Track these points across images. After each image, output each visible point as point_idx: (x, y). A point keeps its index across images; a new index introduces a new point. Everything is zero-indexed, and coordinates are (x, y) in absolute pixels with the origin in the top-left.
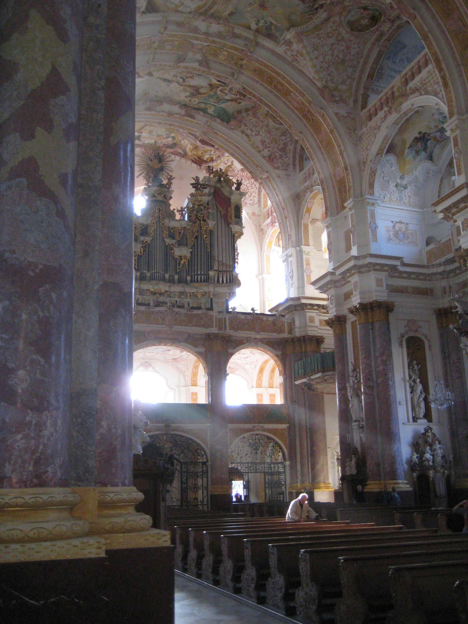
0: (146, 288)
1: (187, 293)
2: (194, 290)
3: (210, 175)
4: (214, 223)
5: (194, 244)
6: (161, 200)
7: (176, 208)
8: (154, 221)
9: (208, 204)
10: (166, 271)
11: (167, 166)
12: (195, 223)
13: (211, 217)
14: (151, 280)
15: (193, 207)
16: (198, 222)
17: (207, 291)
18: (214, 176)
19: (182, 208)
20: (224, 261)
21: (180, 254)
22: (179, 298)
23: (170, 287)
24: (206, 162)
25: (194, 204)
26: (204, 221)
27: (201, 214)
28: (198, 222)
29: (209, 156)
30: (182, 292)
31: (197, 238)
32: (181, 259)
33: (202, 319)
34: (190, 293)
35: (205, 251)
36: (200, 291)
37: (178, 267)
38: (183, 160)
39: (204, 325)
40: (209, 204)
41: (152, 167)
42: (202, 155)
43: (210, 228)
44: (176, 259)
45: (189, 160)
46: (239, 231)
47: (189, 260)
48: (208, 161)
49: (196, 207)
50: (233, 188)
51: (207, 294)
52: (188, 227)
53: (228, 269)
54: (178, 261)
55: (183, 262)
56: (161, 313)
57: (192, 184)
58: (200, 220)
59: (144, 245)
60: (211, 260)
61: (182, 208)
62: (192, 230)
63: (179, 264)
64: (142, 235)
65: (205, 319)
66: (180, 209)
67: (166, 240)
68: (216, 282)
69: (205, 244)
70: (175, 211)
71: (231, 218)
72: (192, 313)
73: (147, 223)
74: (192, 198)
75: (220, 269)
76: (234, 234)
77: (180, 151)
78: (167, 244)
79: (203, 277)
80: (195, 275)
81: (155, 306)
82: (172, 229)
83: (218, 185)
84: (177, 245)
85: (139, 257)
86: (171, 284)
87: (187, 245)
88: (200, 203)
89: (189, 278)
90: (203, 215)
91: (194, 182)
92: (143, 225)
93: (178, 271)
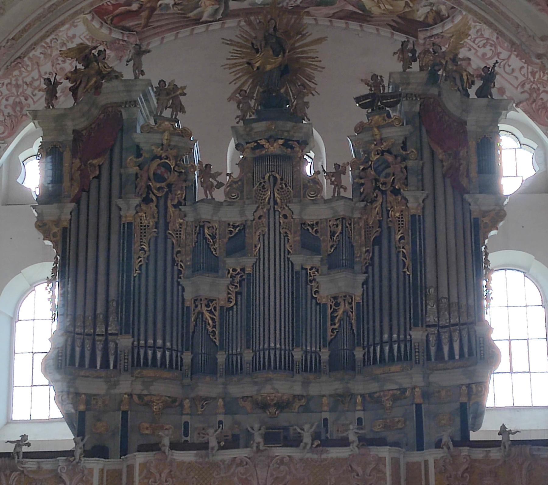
0: (241, 395)
1: (352, 396)
2: (373, 387)
3: (407, 64)
4: (421, 195)
5: (372, 259)
6: (278, 152)
7: (321, 170)
8: (260, 212)
9: (404, 148)
10: (296, 343)
11: (307, 58)
12: (372, 202)
13: (412, 180)
14: (254, 369)
15: (368, 159)
17: (405, 386)
18: (421, 69)
19: (337, 166)
20: (454, 299)
21: (334, 291)
22: (330, 411)
23: (306, 383)
24: (425, 25)
25: (367, 152)
26: (396, 192)
27: (387, 176)
28: (380, 199)
29: (427, 9)
30: (339, 395)
31: (378, 241)
32: (337, 304)
33: (352, 470)
34: (362, 396)
36: (386, 388)
37: (329, 328)
38: (369, 28)
40: (408, 144)
41: (258, 68)
42: (407, 10)
43: (413, 212)
44: (325, 305)
45: (379, 25)
46: (492, 208)
47: (358, 304)
48: (430, 20)
49: (374, 158)
50: (472, 92)
51: (408, 393)
52: (357, 215)
53: (464, 319)
54: (329, 311)
55: (341, 312)
56: (241, 464)
57: (358, 100)
59: (238, 278)
60: (415, 299)
61: (337, 166)
62: (366, 223)
63: (333, 318)
64: (230, 253)
67: (293, 258)
68: (433, 359)
71: (468, 176)
72: (324, 456)
73: (244, 219)
74: (361, 136)
75: (442, 323)
76: (476, 220)
77: (351, 8)
78: (297, 268)
79: (396, 346)
80: (375, 345)
81: (221, 448)
82: (312, 226)
83: (434, 91)
84: (325, 269)
85: (225, 311)
86: (311, 376)
87: (351, 266)
88: (383, 147)
89: (359, 353)
91: (365, 90)
92: (234, 227)
93: (329, 338)
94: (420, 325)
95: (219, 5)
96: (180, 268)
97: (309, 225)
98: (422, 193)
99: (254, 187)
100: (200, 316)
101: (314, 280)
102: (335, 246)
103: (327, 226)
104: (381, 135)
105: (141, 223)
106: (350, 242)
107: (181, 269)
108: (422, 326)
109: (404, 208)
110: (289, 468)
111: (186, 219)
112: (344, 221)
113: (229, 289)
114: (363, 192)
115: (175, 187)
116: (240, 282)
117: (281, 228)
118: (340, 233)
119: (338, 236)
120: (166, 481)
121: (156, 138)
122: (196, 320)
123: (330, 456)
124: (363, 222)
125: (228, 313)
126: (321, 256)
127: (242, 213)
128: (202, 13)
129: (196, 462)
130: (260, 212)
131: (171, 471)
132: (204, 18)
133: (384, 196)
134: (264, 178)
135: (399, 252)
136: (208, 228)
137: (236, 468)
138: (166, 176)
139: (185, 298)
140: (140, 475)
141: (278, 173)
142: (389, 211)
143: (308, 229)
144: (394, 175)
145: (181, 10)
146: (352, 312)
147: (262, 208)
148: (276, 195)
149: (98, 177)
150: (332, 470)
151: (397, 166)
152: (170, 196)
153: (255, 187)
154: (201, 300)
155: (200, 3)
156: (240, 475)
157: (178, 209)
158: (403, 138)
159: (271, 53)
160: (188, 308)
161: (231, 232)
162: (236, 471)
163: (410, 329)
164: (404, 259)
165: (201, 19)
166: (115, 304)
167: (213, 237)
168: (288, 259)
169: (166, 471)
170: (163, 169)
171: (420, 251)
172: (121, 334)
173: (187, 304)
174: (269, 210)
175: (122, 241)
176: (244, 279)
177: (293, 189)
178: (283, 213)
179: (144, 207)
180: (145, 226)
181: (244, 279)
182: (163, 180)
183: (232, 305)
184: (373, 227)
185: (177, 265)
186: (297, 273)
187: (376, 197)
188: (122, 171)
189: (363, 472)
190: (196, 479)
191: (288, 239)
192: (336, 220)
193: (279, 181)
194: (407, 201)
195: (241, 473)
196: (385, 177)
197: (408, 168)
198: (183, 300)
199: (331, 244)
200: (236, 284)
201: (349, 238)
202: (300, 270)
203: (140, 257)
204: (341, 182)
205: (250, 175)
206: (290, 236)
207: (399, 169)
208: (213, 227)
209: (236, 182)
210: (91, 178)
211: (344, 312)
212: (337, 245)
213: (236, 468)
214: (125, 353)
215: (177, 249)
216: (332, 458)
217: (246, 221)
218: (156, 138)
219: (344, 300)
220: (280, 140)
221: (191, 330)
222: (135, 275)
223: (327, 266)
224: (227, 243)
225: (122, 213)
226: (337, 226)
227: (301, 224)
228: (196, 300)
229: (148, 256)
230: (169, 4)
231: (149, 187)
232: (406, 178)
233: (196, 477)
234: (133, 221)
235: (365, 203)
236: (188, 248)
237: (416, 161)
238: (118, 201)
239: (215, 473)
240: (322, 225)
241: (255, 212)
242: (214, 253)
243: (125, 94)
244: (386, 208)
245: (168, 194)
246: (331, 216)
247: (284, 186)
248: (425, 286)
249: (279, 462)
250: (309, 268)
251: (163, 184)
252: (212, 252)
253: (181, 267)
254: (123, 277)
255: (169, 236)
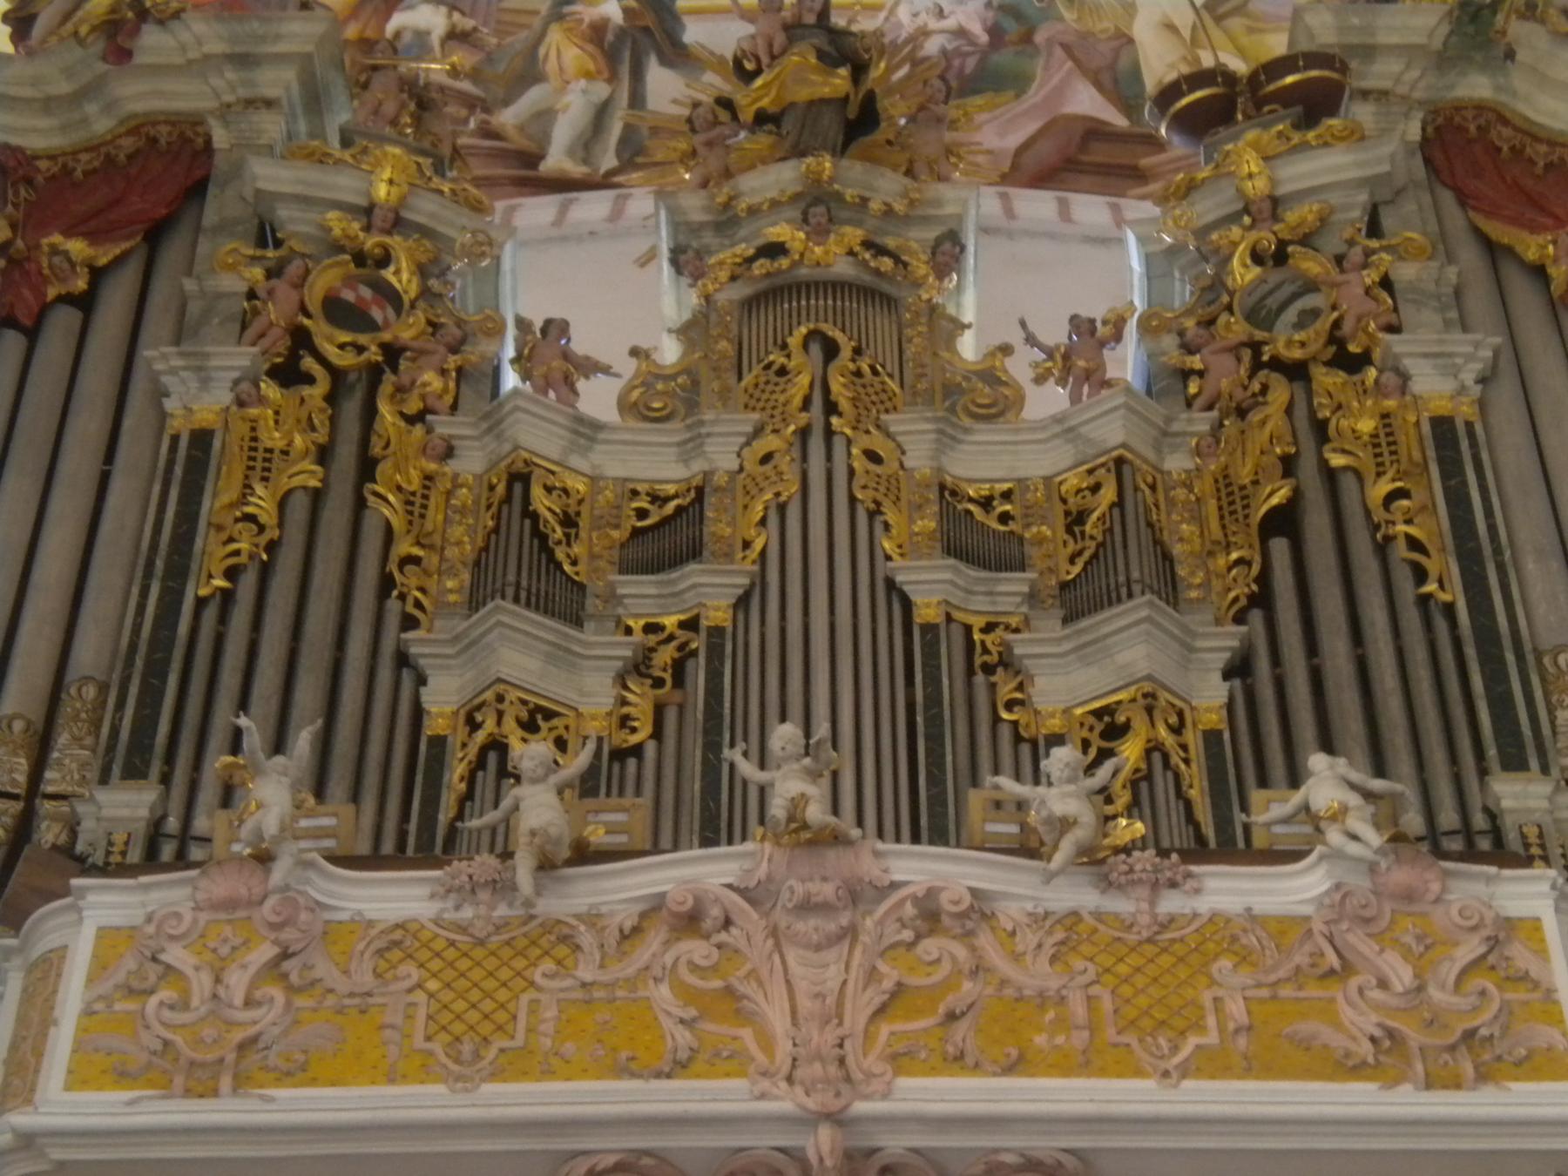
5: (1264, 578)
6: (843, 268)
8: (770, 442)
9: (1374, 229)
12: (1242, 413)
15: (1214, 289)
16: (1280, 393)
19: (1081, 326)
31: (1284, 521)
35: (1411, 618)
39: (1389, 1042)
40: (1388, 221)
47: (1212, 738)
49: (1242, 273)
58: (1297, 372)
59: (666, 655)
62: (1224, 480)
65: (1402, 975)
66: (1056, 334)
69: (1401, 550)
70: (1020, 368)
73: (698, 466)
77: (1087, 102)
78: (927, 610)
82: (986, 503)
87: (1170, 588)
90: (1324, 323)
92: (658, 499)
94: (1534, 763)
95: (610, 81)
96: (410, 609)
97: (971, 500)
98: (1477, 345)
99: (740, 378)
100: (492, 757)
101: (1006, 661)
102: (1087, 555)
103: (1049, 498)
104: (1273, 182)
105: (254, 439)
106: (1157, 542)
107: (417, 613)
108: (1545, 770)
109: (1390, 404)
110: (973, 949)
111: (452, 466)
112: (1126, 469)
113: (625, 687)
114: (1196, 396)
115: (413, 360)
116: (679, 668)
117: (859, 480)
118: (1112, 506)
119: (1101, 518)
120: (249, 1003)
121: (344, 185)
122: (471, 780)
123: (1205, 905)
124: (1209, 480)
125: (616, 767)
126: (1031, 575)
127: (692, 446)
128: (545, 117)
129: (437, 922)
130: (770, 442)
131: (285, 955)
132: (556, 160)
133: (1298, 388)
134: (784, 346)
135: (1389, 539)
136: (549, 489)
137: (667, 944)
138: (377, 314)
139: (426, 706)
140: (90, 980)
141: (843, 330)
142: (1325, 422)
143: (968, 512)
144: (1334, 308)
145: (475, 75)
146: (1187, 761)
147: (775, 431)
148: (835, 387)
149: (85, 303)
150: (1225, 963)
151: (1351, 276)
152: (389, 379)
153: (748, 379)
154: (500, 698)
155: (542, 51)
156: (692, 980)
157: (418, 430)
158: (1363, 197)
159: (813, 60)
160: (439, 743)
161: (642, 514)
162: (669, 959)
163: (1483, 772)
164: (1416, 556)
165: (541, 157)
166: (90, 692)
167: (569, 521)
168: (891, 584)
169: (265, 952)
170: (366, 293)
171: (1492, 528)
172: (104, 779)
173: (435, 725)
174: (804, 433)
175: (157, 488)
176: (694, 653)
177: (902, 386)
178: (863, 442)
179: (270, 390)
180: (270, 451)
181: (694, 653)
182: (371, 326)
183: (634, 739)
184: (1255, 483)
185: (402, 597)
186: (929, 629)
187: (1265, 389)
188: (189, 285)
189: (1416, 976)
190: (431, 995)
191: (887, 526)
192: (1090, 472)
193: (846, 352)
194: (1405, 377)
195: (694, 967)
196: (1300, 325)
197: (1397, 286)
198: (418, 713)
199: (1071, 547)
200: (657, 673)
201: (1150, 525)
202: (941, 620)
203: (231, 540)
204: (1101, 367)
205: (723, 345)
206: (890, 515)
207: (1360, 291)
208: (565, 491)
209: (666, 378)
210: (52, 293)
211: (1148, 752)
212: (1099, 545)
213: (667, 944)
214: (110, 844)
215: (404, 547)
216: (1213, 917)
217: (707, 475)
218: (344, 185)
219: (1149, 710)
220: (848, 230)
221: (445, 816)
222: (203, 592)
223: (1060, 613)
224: (622, 546)
225: (170, 405)
226: (1095, 489)
227: (942, 487)
228: (479, 707)
229: (272, 547)
230: (428, 33)
231: (301, 339)
232: (1396, 310)
233: (433, 985)
234: (218, 426)
235: (1215, 414)
236: (452, 552)
237: (1434, 264)
238: (157, 355)
239: (548, 965)
240: (1029, 496)
241: (748, 444)
242: (567, 568)
243: (230, 75)
244: (1312, 412)
245: (382, 372)
246: (1068, 462)
247: (866, 369)
248: (1535, 650)
249: (909, 910)
250: (978, 622)
251: (363, 339)
252: (559, 566)
253: (418, 605)
254: (144, 593)
255: (371, 500)
